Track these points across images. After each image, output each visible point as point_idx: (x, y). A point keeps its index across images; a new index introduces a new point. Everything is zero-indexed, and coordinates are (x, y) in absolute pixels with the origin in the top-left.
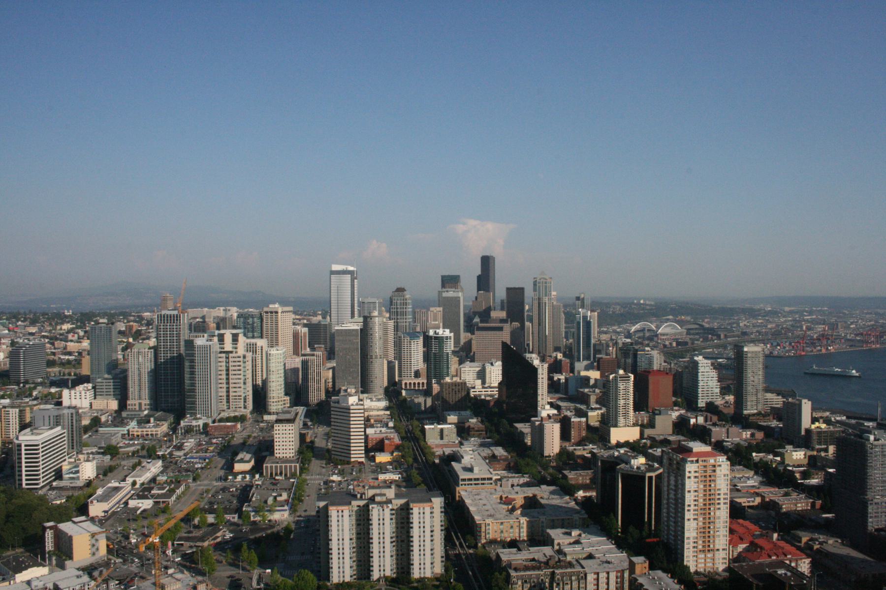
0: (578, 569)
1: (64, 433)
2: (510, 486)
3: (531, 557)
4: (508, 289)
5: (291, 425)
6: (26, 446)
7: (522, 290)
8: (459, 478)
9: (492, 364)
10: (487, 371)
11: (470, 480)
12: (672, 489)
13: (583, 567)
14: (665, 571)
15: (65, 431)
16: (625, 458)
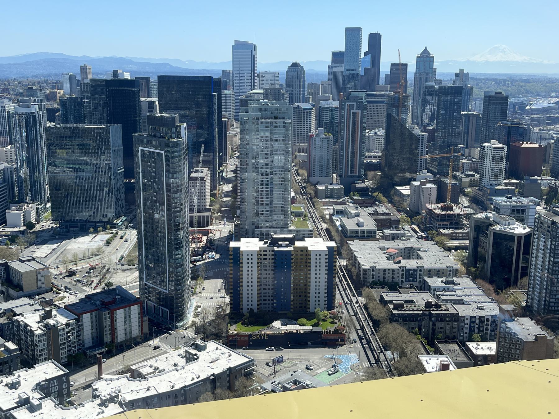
0: (452, 311)
1: (6, 185)
2: (391, 238)
3: (411, 298)
4: (392, 65)
5: (203, 182)
7: (406, 65)
8: (347, 231)
9: (376, 133)
10: (371, 139)
11: (357, 232)
12: (541, 249)
13: (457, 311)
14: (532, 319)
15: (6, 184)
16: (498, 220)
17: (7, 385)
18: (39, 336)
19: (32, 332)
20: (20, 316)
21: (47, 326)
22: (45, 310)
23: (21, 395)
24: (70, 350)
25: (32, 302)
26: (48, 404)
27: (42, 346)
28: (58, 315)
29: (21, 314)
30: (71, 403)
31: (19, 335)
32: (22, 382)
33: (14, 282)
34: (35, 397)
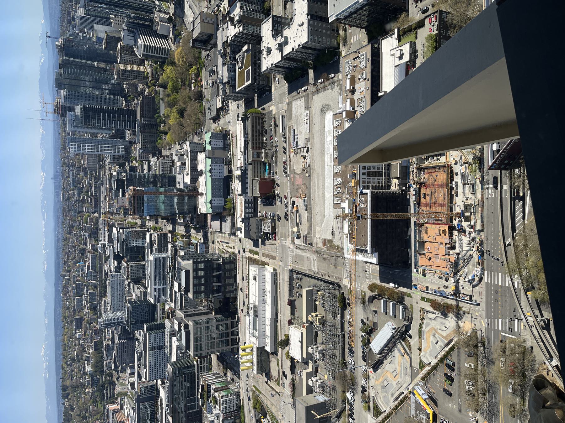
6: (144, 51)
17: (267, 55)
18: (244, 29)
19: (239, 33)
20: (228, 38)
21: (239, 22)
22: (228, 21)
23: (276, 48)
24: (259, 11)
25: (221, 29)
26: (287, 32)
27: (250, 29)
28: (234, 13)
29: (228, 37)
30: (291, 19)
31: (240, 42)
32: (269, 46)
33: (207, 38)
34: (280, 40)
